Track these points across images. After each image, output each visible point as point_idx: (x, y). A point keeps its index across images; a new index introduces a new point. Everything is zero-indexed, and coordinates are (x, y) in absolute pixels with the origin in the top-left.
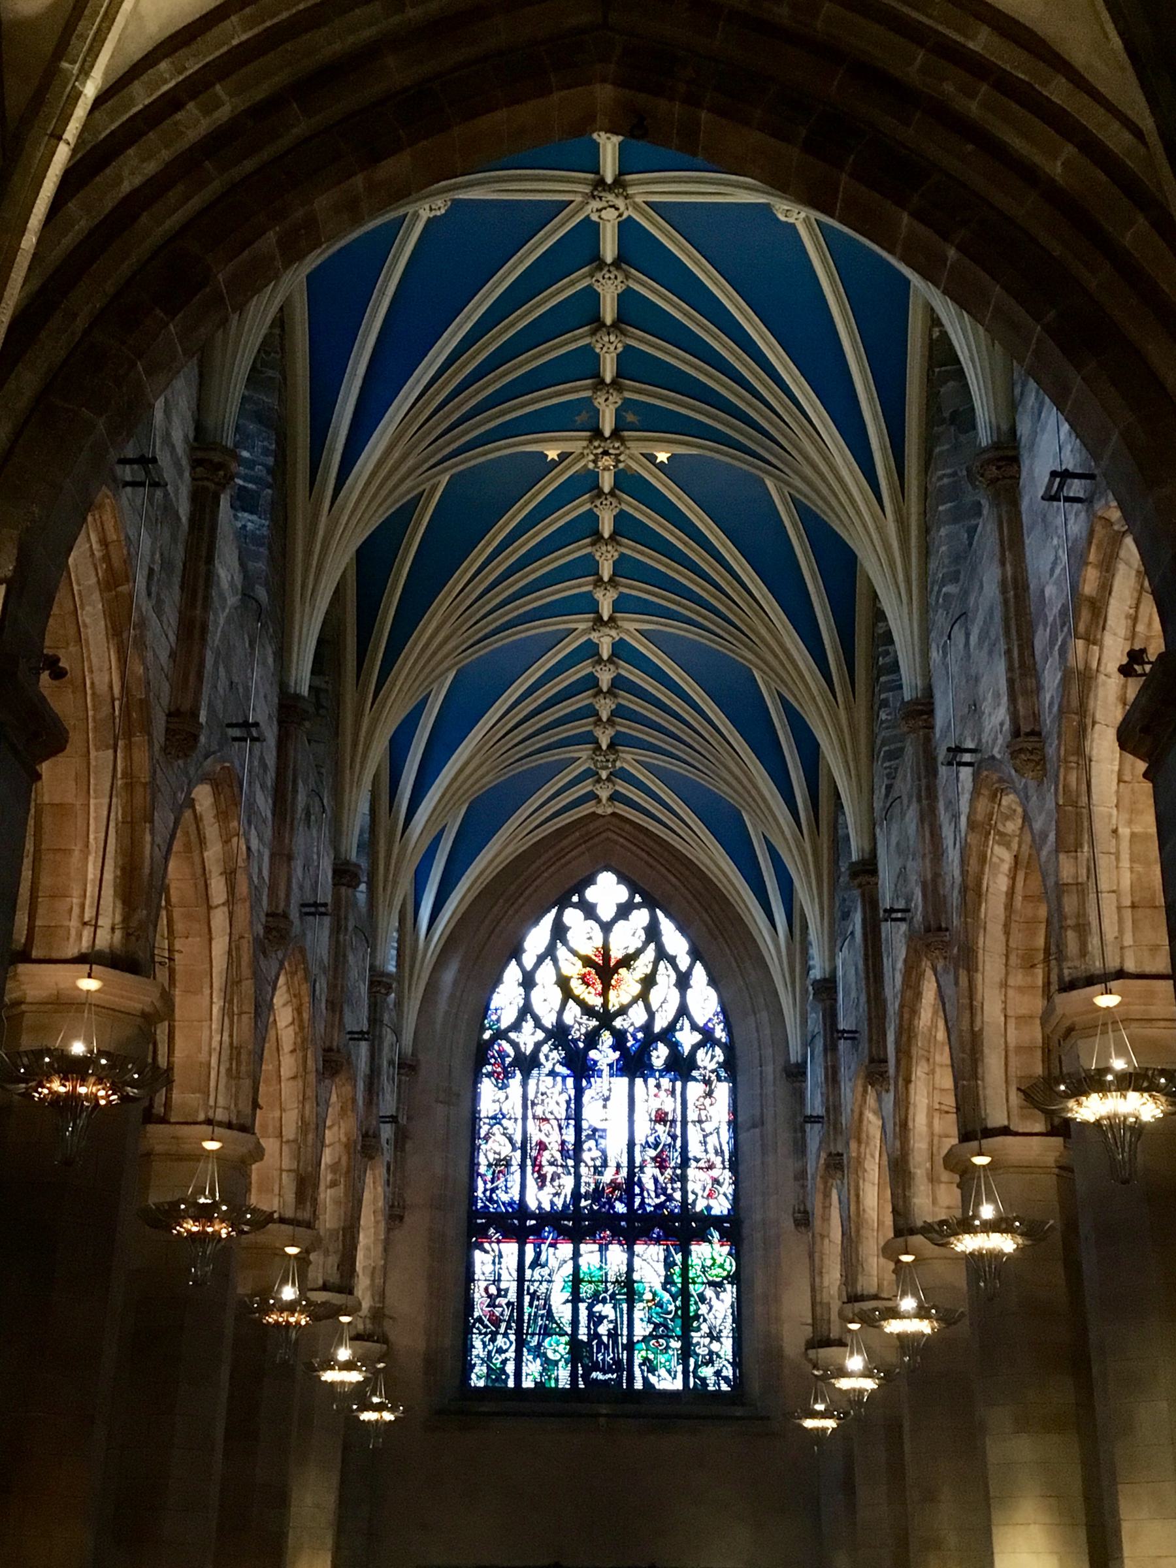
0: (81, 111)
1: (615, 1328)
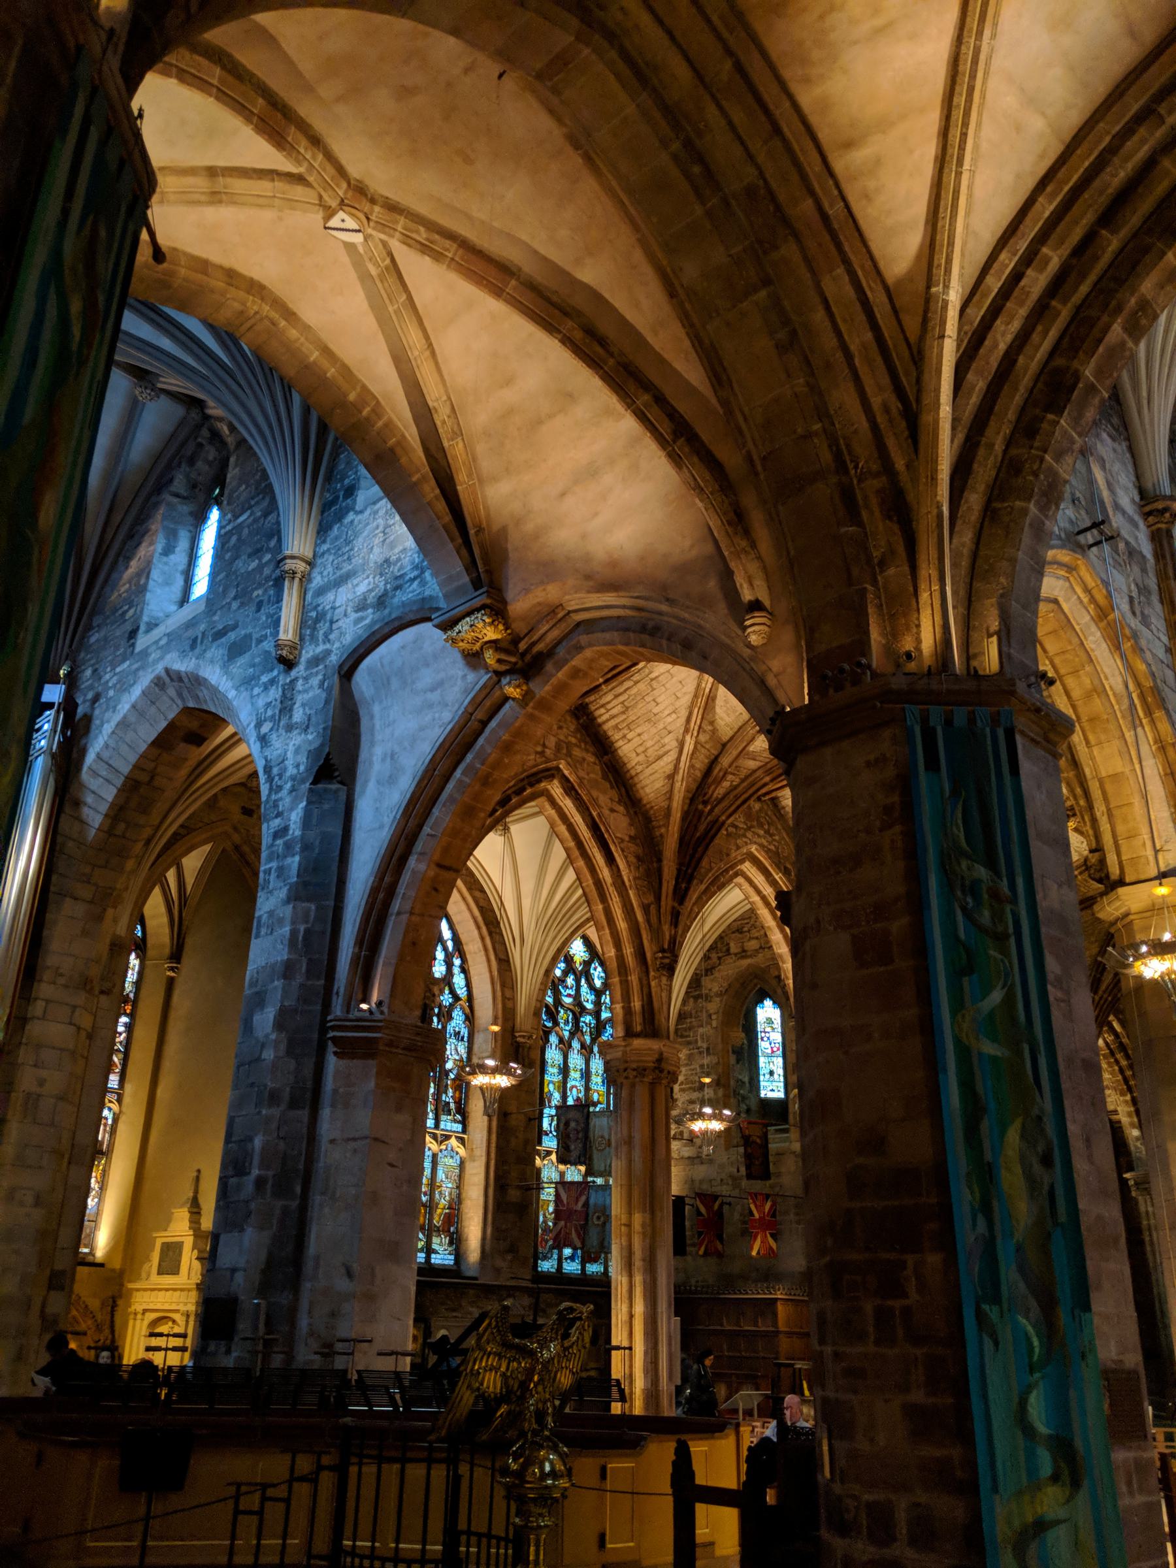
0: (952, 314)
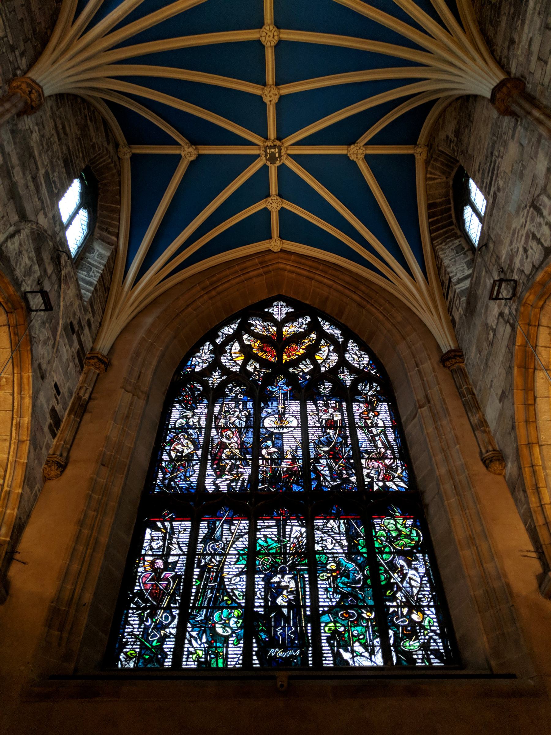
1: (297, 599)
